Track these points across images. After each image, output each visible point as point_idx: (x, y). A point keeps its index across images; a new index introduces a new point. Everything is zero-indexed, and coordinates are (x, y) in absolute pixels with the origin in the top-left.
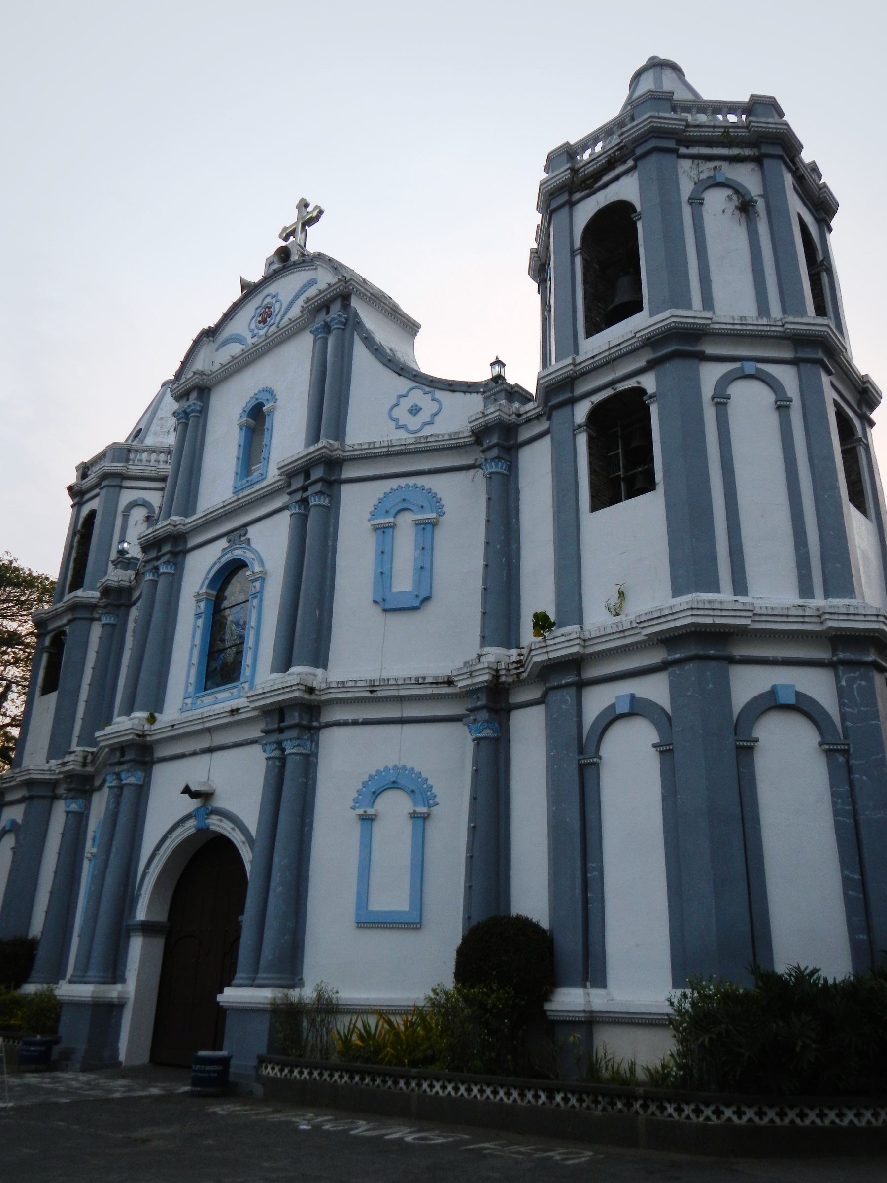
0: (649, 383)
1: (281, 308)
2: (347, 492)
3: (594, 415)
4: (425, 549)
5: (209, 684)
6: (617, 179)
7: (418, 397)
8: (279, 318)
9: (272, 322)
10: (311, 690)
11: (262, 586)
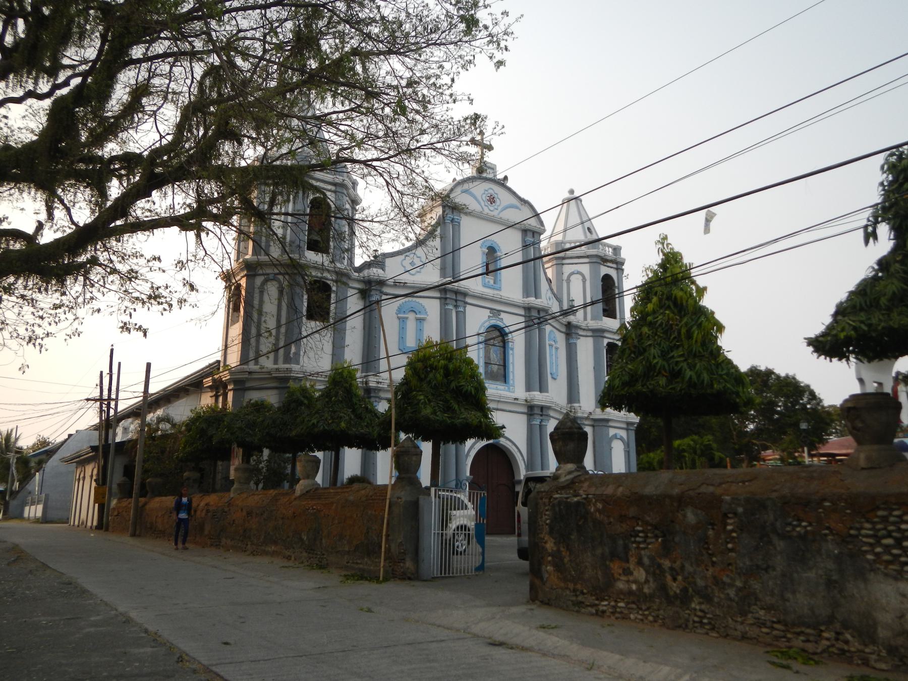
3: (609, 344)
6: (611, 267)
8: (500, 208)
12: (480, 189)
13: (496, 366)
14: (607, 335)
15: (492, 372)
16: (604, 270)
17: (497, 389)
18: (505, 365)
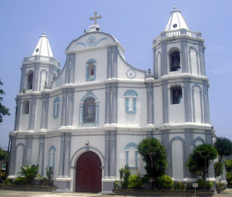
0: (182, 85)
1: (96, 41)
2: (119, 89)
5: (85, 121)
8: (96, 43)
9: (94, 44)
10: (117, 128)
11: (98, 104)
13: (91, 116)
14: (169, 81)
15: (88, 118)
16: (170, 47)
17: (88, 126)
18: (94, 115)
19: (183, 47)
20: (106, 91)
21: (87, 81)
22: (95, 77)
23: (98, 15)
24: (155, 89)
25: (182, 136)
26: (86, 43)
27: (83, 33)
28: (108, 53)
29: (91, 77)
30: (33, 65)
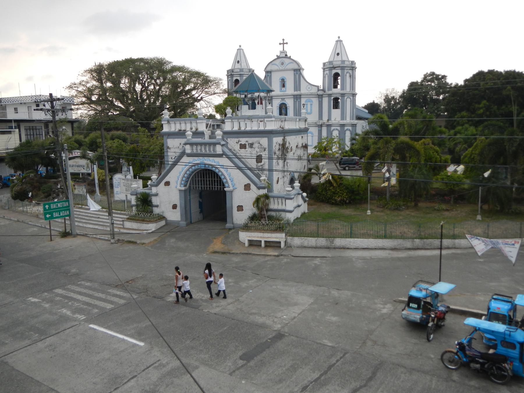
3: (334, 99)
4: (311, 107)
7: (309, 86)
12: (278, 62)
14: (332, 95)
16: (334, 71)
19: (343, 73)
20: (294, 100)
21: (280, 91)
22: (286, 89)
23: (285, 42)
24: (324, 99)
25: (339, 128)
26: (278, 65)
27: (276, 57)
28: (294, 74)
29: (283, 89)
30: (239, 75)
